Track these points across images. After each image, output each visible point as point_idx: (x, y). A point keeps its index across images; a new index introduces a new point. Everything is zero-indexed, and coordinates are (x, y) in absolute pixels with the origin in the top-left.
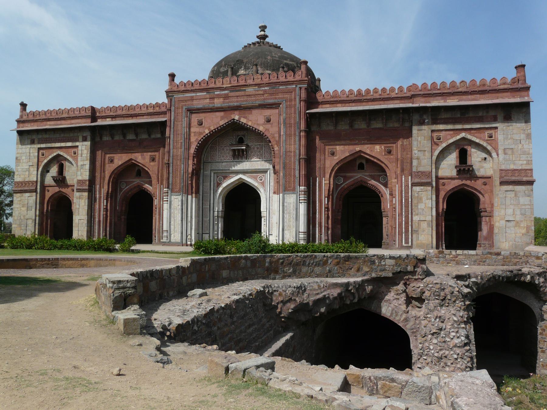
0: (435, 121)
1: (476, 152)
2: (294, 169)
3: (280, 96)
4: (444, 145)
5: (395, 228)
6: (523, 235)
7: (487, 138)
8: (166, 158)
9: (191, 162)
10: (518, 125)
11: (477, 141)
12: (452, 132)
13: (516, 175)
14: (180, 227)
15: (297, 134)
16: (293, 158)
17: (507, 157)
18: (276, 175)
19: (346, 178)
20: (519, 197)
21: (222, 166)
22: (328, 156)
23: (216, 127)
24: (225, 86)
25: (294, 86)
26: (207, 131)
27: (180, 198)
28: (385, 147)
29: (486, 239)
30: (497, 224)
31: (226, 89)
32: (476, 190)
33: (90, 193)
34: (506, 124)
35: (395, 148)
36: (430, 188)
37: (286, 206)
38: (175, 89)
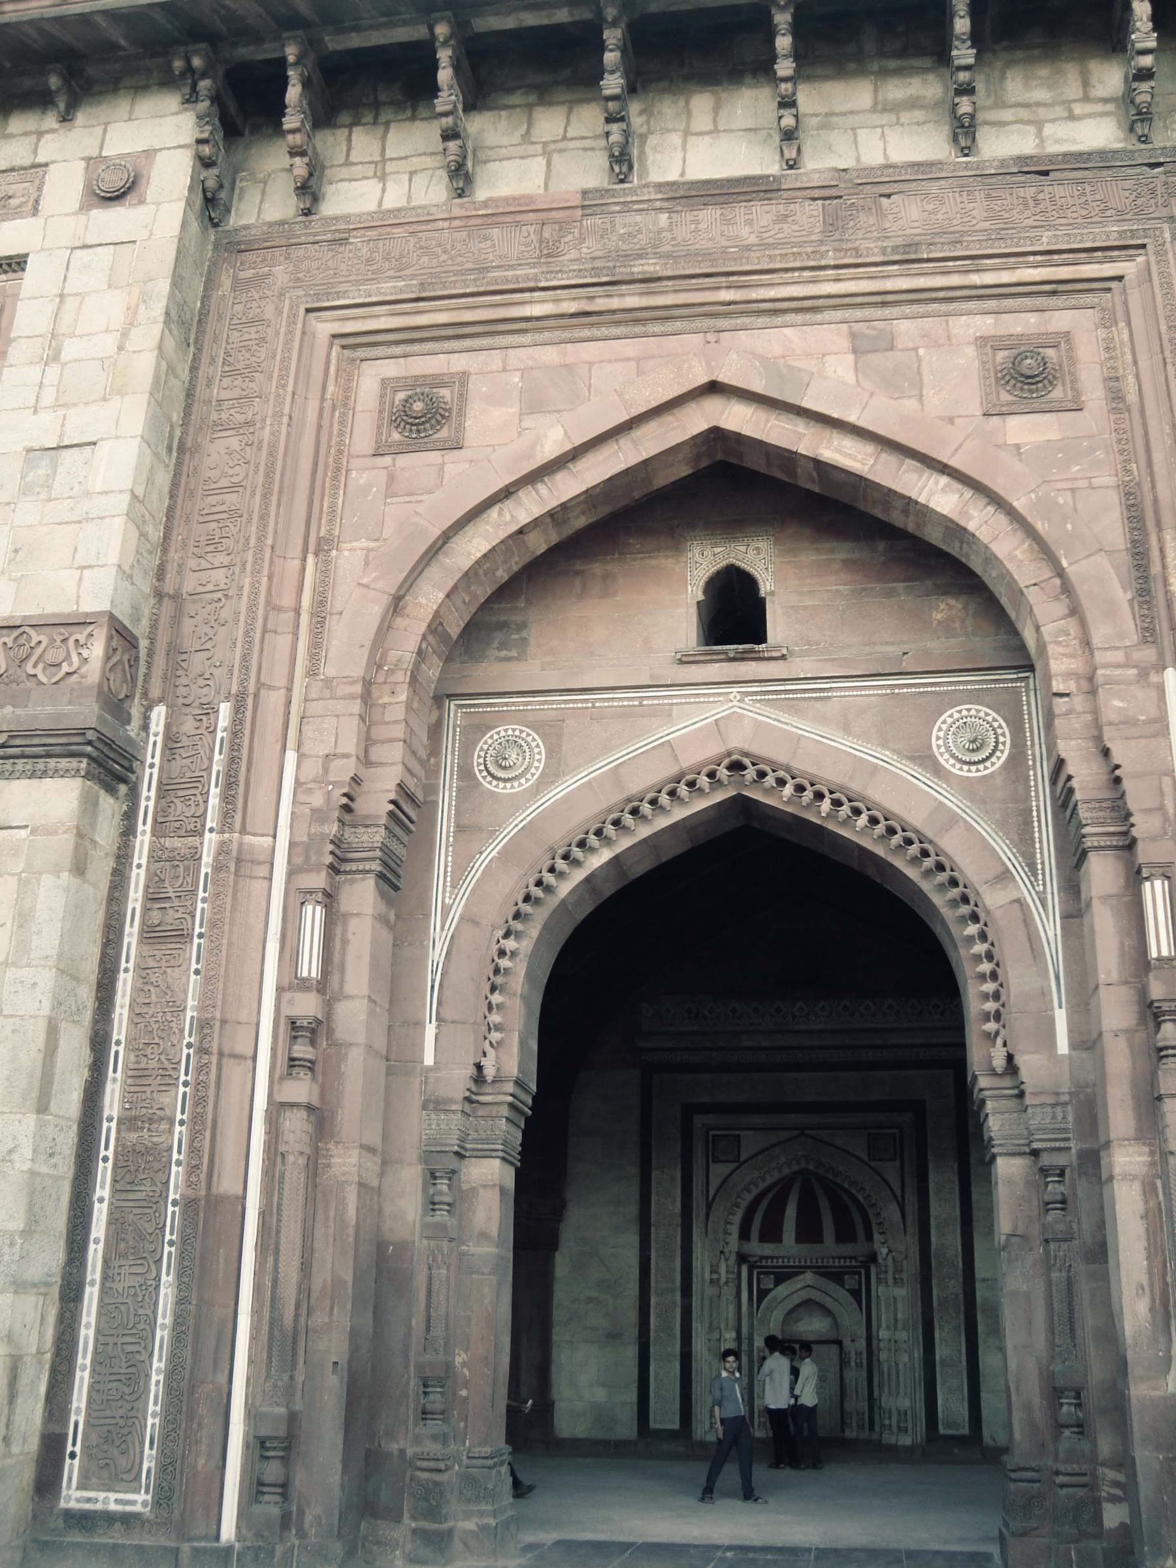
33: (110, 807)
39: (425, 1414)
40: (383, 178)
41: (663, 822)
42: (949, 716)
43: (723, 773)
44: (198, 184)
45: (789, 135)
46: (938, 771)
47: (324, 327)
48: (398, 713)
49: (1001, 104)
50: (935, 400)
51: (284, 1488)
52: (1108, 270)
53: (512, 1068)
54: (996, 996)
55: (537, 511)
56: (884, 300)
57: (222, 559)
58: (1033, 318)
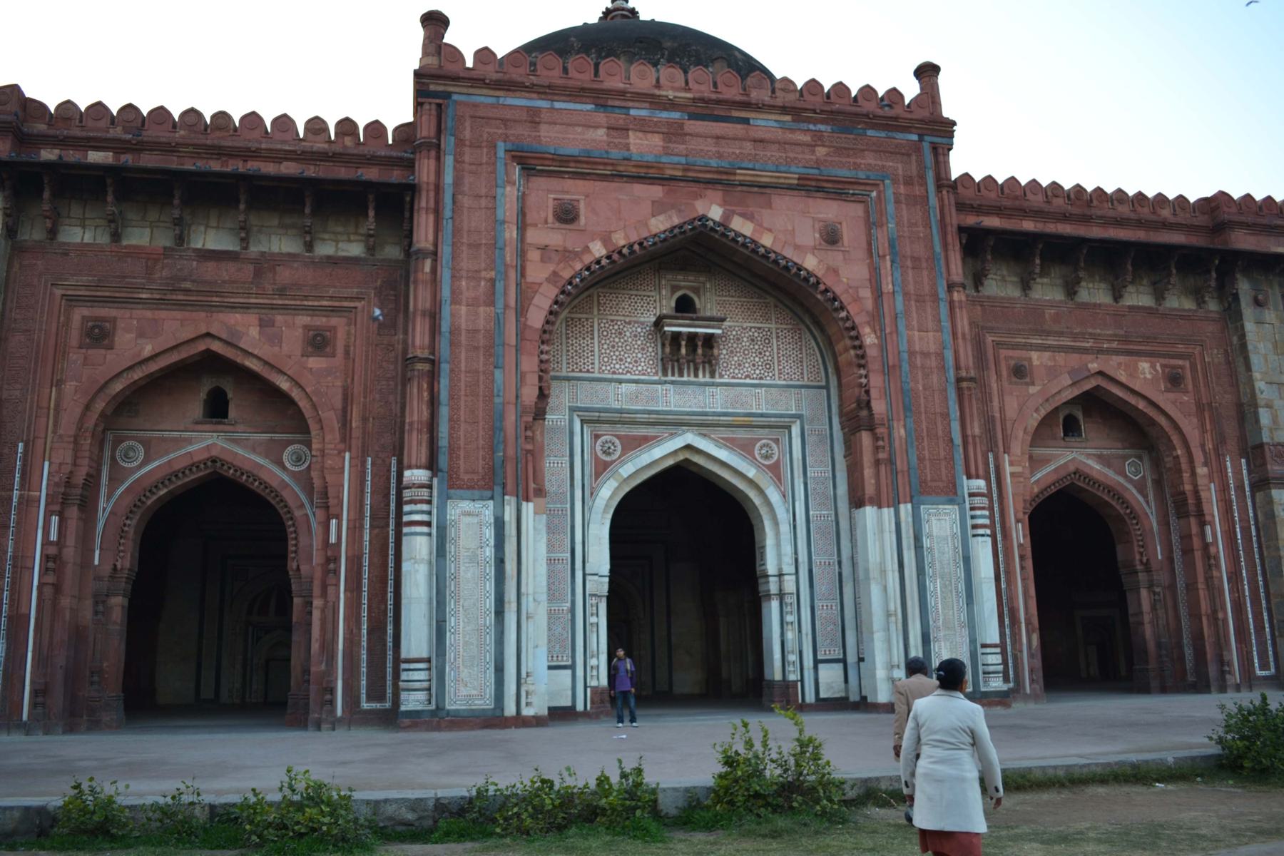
2: (946, 416)
3: (870, 159)
5: (1225, 620)
8: (419, 336)
9: (530, 364)
14: (490, 639)
15: (942, 293)
16: (935, 378)
18: (866, 438)
19: (1035, 463)
21: (621, 397)
22: (1011, 383)
23: (634, 237)
24: (671, 94)
25: (915, 137)
26: (598, 250)
27: (487, 511)
28: (1162, 366)
31: (671, 105)
37: (931, 549)
38: (450, 68)
39: (92, 683)
40: (84, 227)
41: (187, 480)
42: (290, 449)
43: (209, 464)
44: (6, 225)
45: (242, 240)
46: (284, 468)
47: (58, 292)
48: (87, 447)
49: (325, 231)
50: (285, 348)
51: (43, 704)
52: (352, 304)
53: (128, 565)
54: (296, 545)
55: (141, 375)
56: (273, 307)
57: (18, 386)
58: (324, 319)
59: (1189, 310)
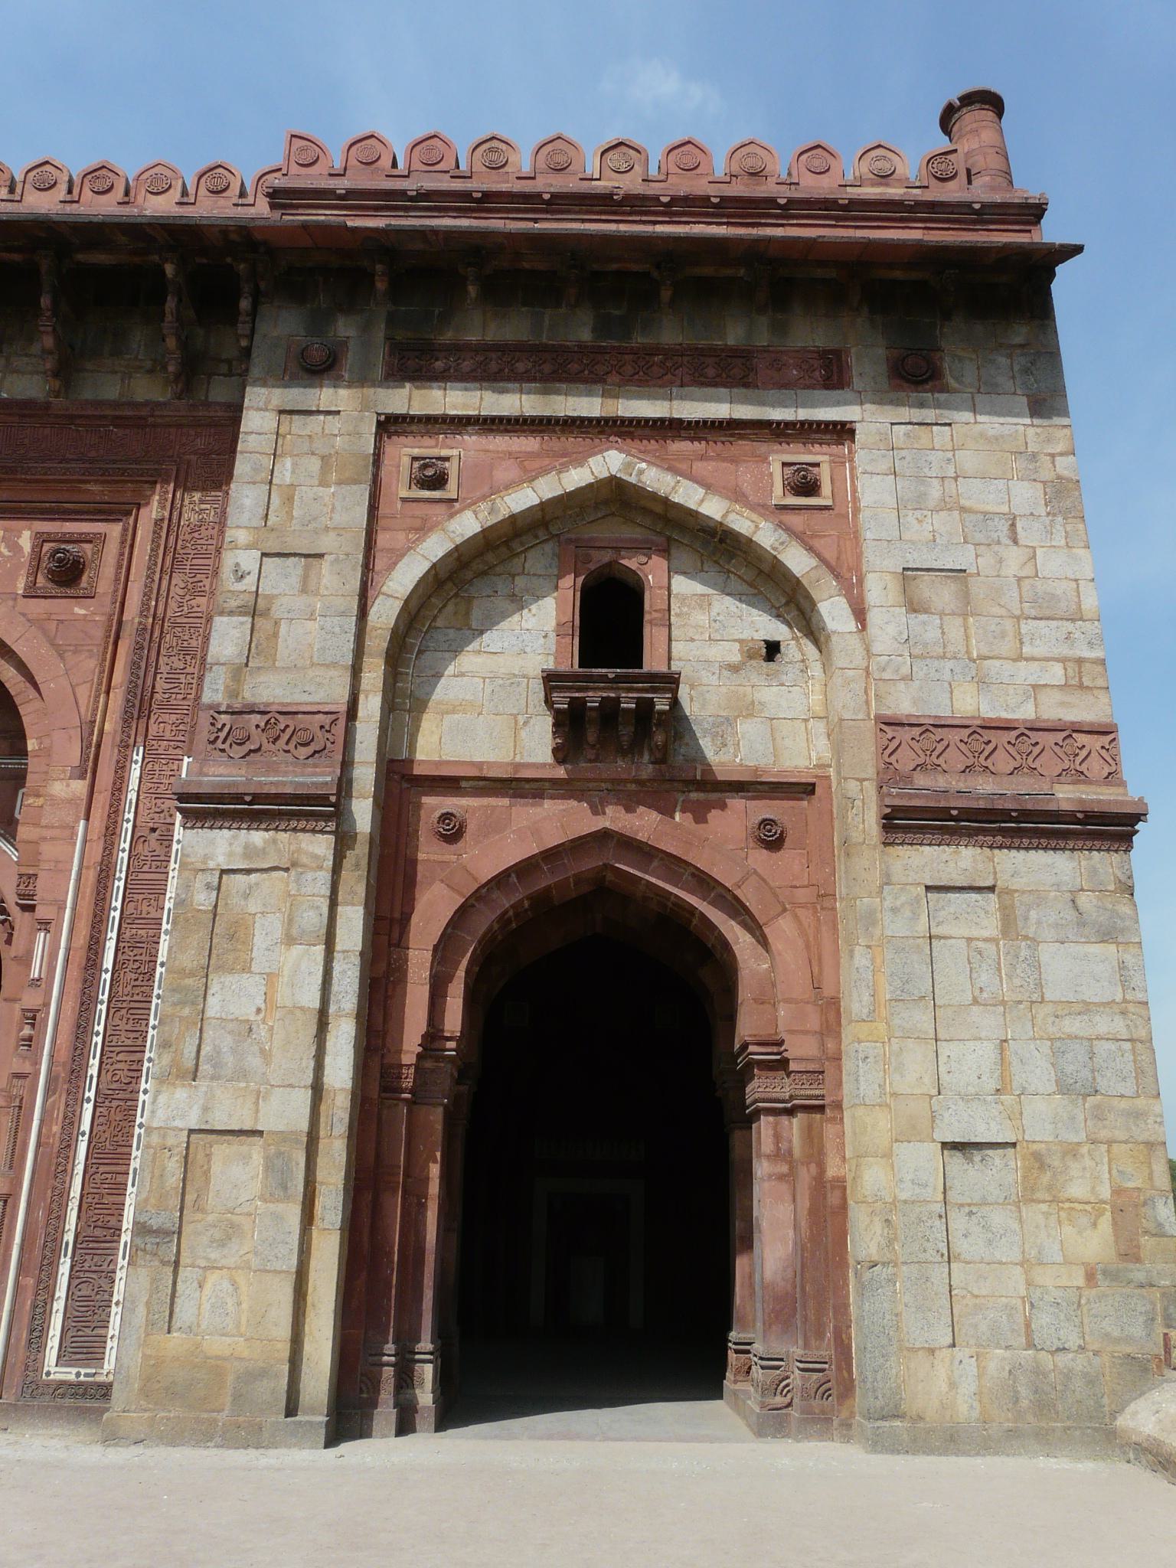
0: (413, 362)
1: (704, 602)
4: (467, 525)
6: (1090, 1277)
7: (778, 494)
10: (990, 424)
11: (713, 508)
12: (529, 443)
13: (1002, 762)
17: (928, 629)
20: (1034, 942)
29: (785, 1311)
30: (871, 1181)
32: (704, 883)
34: (905, 413)
35: (112, 549)
36: (320, 846)
59: (146, 403)
